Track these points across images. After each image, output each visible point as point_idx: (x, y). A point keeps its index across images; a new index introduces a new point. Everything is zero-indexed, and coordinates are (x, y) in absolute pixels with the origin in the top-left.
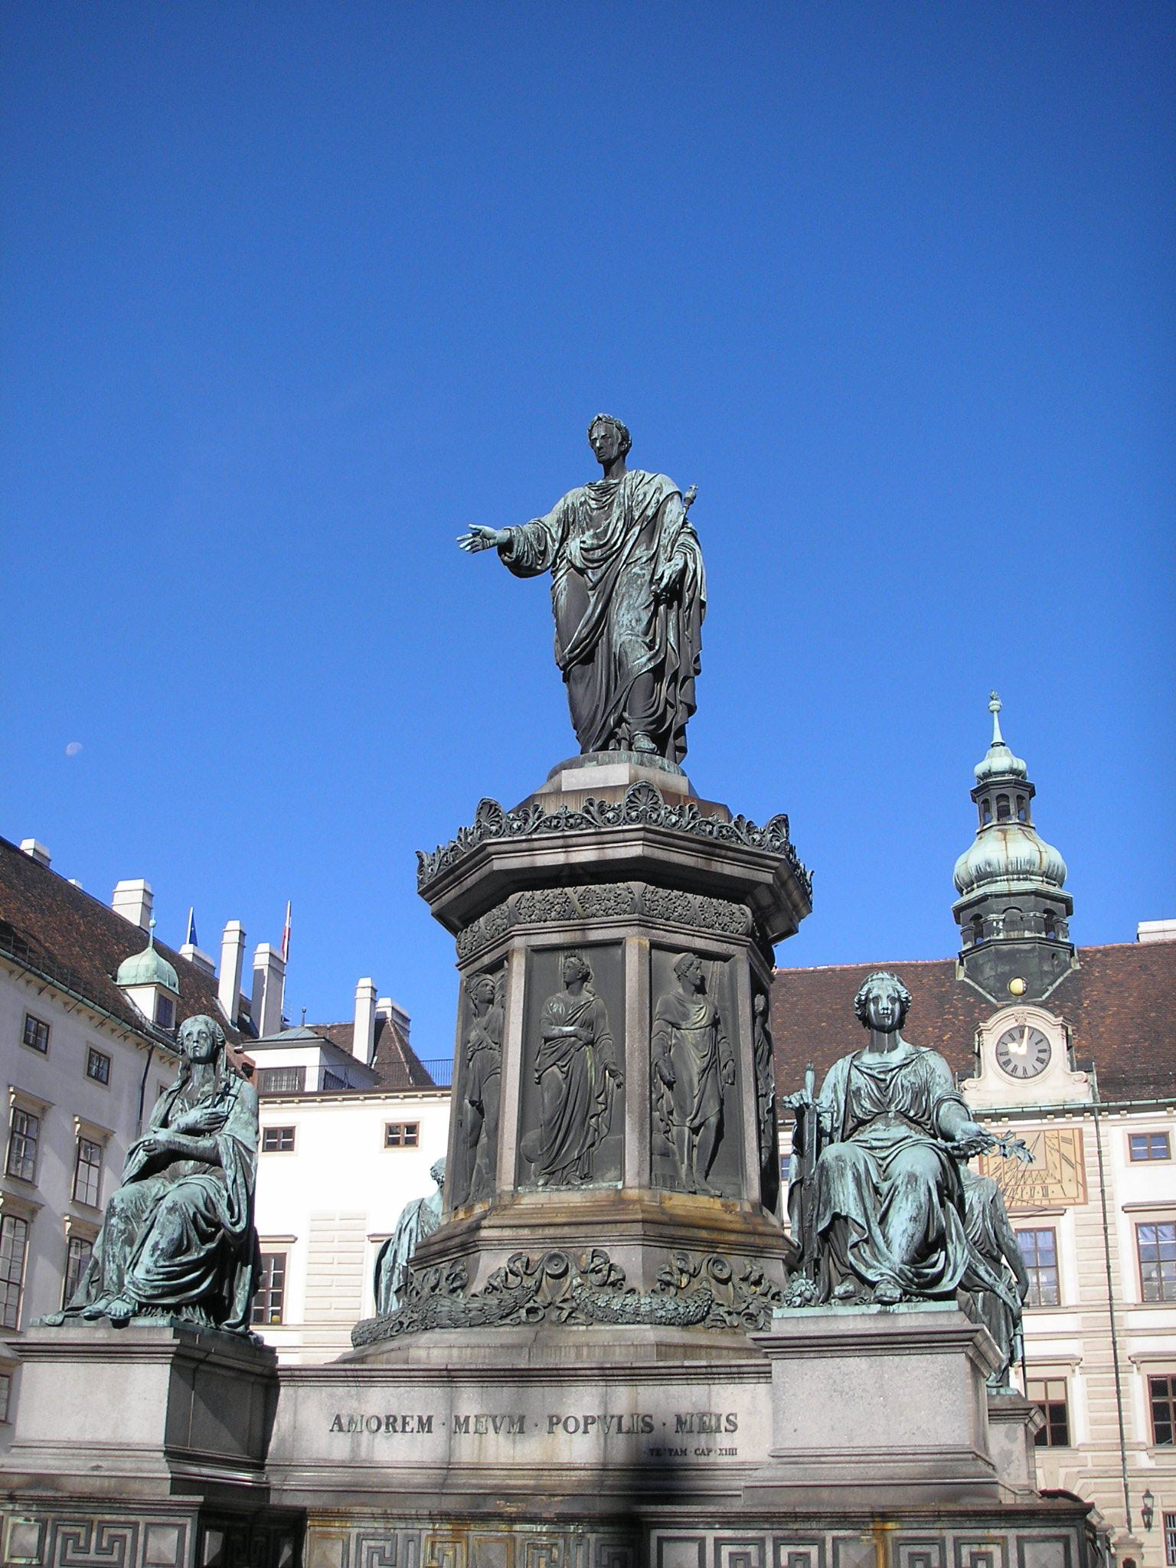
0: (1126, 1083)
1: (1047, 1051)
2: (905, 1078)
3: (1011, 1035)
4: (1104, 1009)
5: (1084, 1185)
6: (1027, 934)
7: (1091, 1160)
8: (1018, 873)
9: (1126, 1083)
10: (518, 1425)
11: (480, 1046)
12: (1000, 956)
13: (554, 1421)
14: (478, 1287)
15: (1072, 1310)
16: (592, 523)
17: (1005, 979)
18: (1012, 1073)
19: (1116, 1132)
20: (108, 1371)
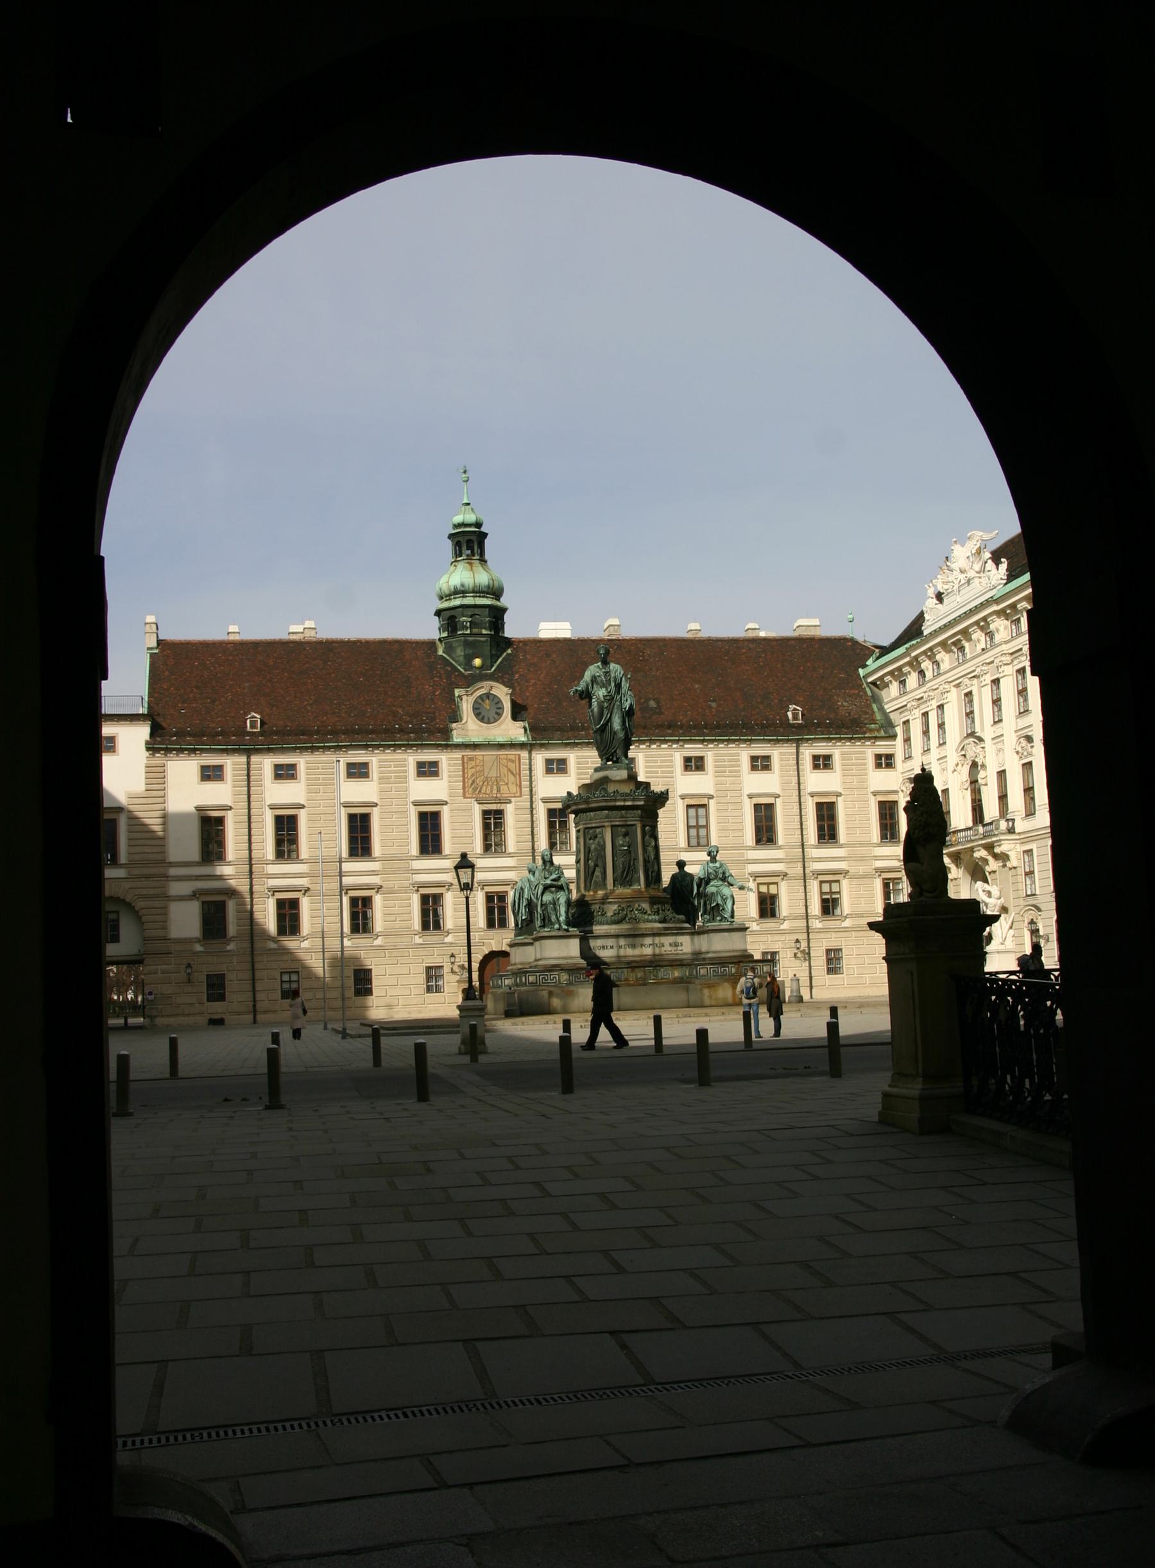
0: (545, 729)
1: (502, 708)
2: (721, 871)
3: (480, 697)
4: (527, 681)
5: (520, 786)
6: (484, 632)
7: (525, 772)
8: (479, 592)
9: (545, 729)
10: (634, 946)
11: (596, 849)
12: (467, 644)
13: (642, 945)
14: (609, 914)
15: (511, 855)
16: (603, 686)
17: (469, 659)
18: (482, 720)
19: (540, 758)
20: (564, 941)
